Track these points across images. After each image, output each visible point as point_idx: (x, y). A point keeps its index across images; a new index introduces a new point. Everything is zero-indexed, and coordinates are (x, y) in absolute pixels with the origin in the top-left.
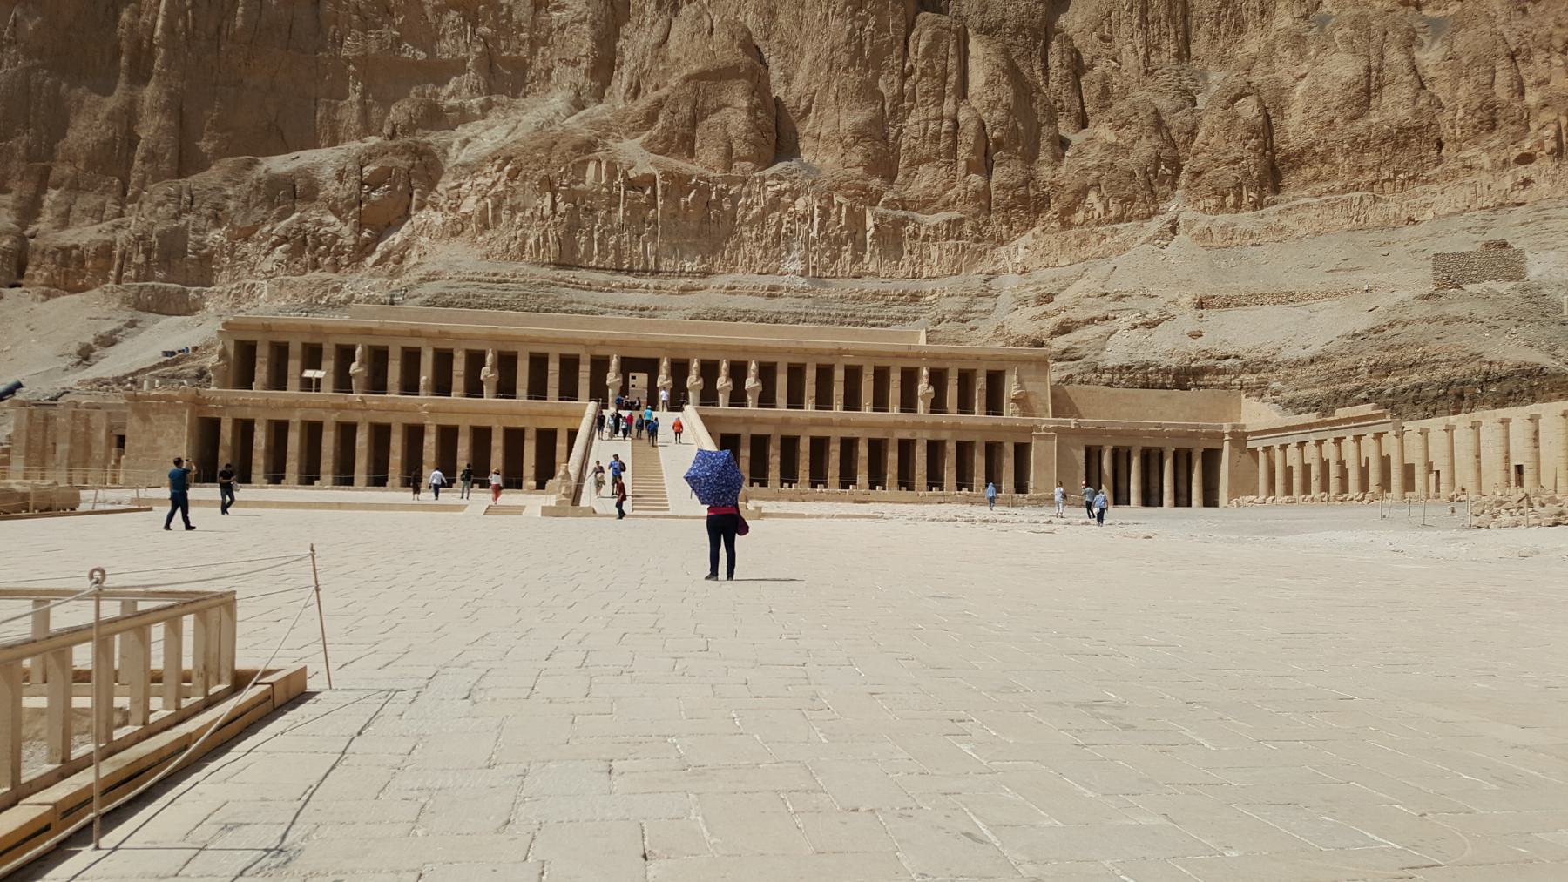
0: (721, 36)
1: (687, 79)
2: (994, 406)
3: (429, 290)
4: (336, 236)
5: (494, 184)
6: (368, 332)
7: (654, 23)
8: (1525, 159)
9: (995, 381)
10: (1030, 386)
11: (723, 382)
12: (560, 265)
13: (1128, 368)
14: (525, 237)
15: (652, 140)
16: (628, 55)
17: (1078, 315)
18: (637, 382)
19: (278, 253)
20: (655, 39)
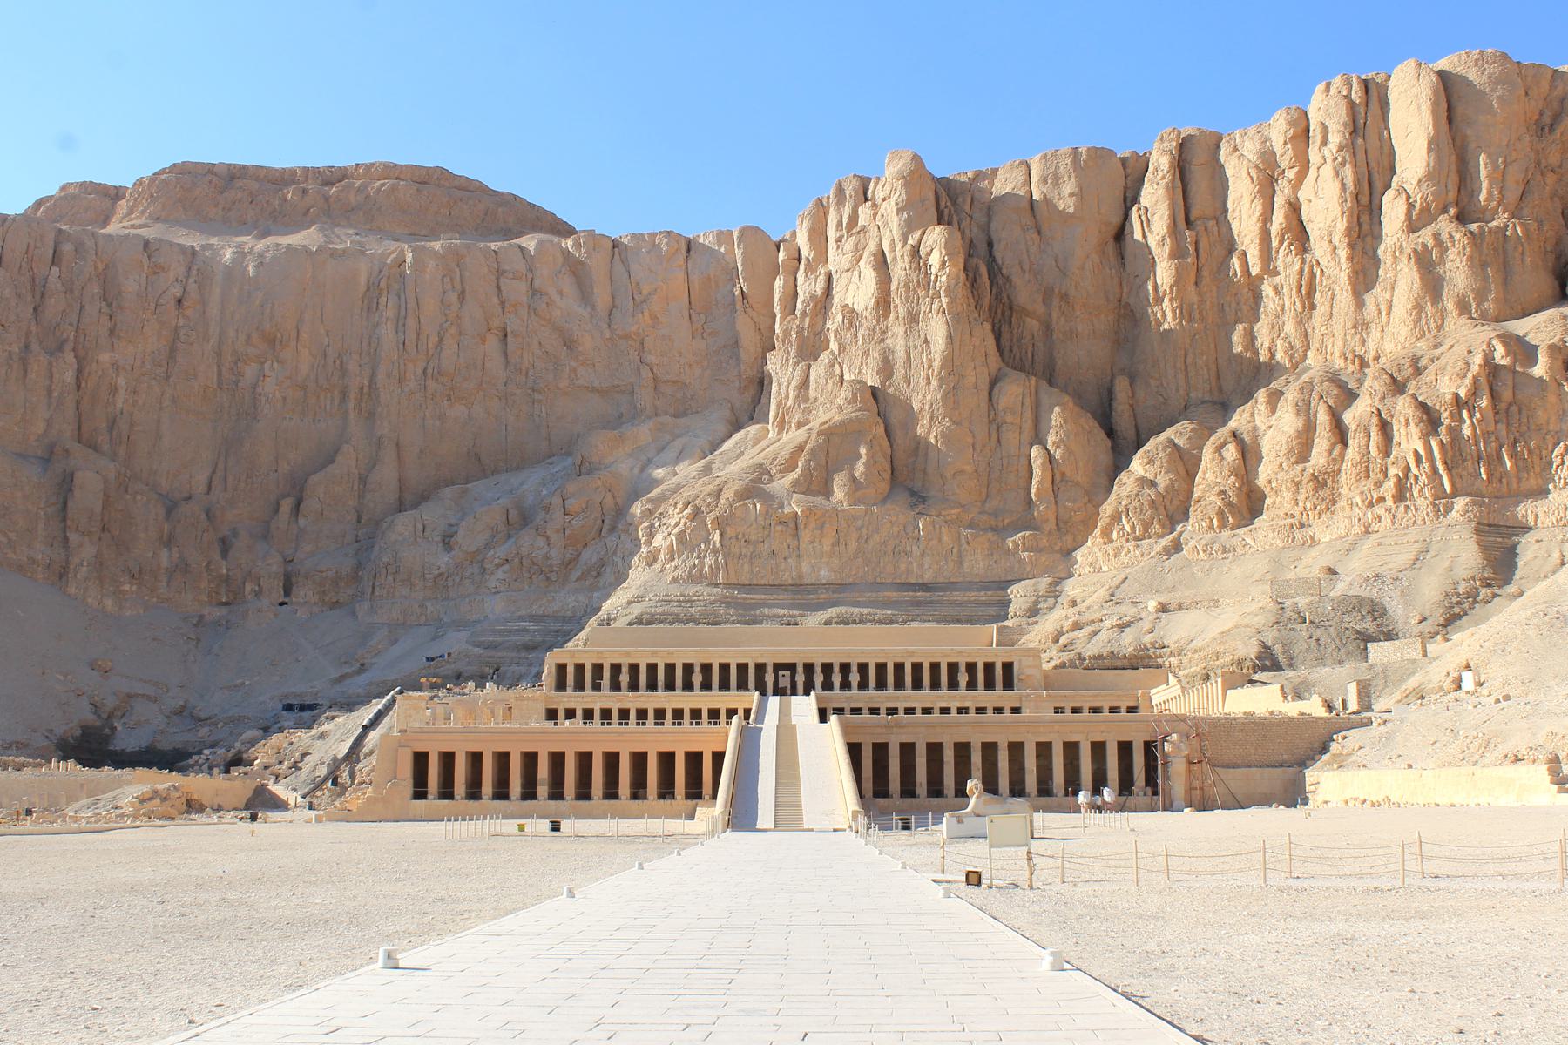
0: (844, 393)
1: (820, 433)
2: (1008, 684)
3: (637, 610)
4: (547, 557)
5: (677, 524)
6: (628, 654)
7: (797, 364)
8: (1382, 500)
9: (1008, 667)
10: (1029, 672)
11: (837, 679)
12: (728, 585)
13: (1100, 657)
14: (702, 564)
15: (795, 483)
16: (774, 389)
17: (1086, 617)
18: (787, 678)
19: (500, 574)
20: (796, 381)
